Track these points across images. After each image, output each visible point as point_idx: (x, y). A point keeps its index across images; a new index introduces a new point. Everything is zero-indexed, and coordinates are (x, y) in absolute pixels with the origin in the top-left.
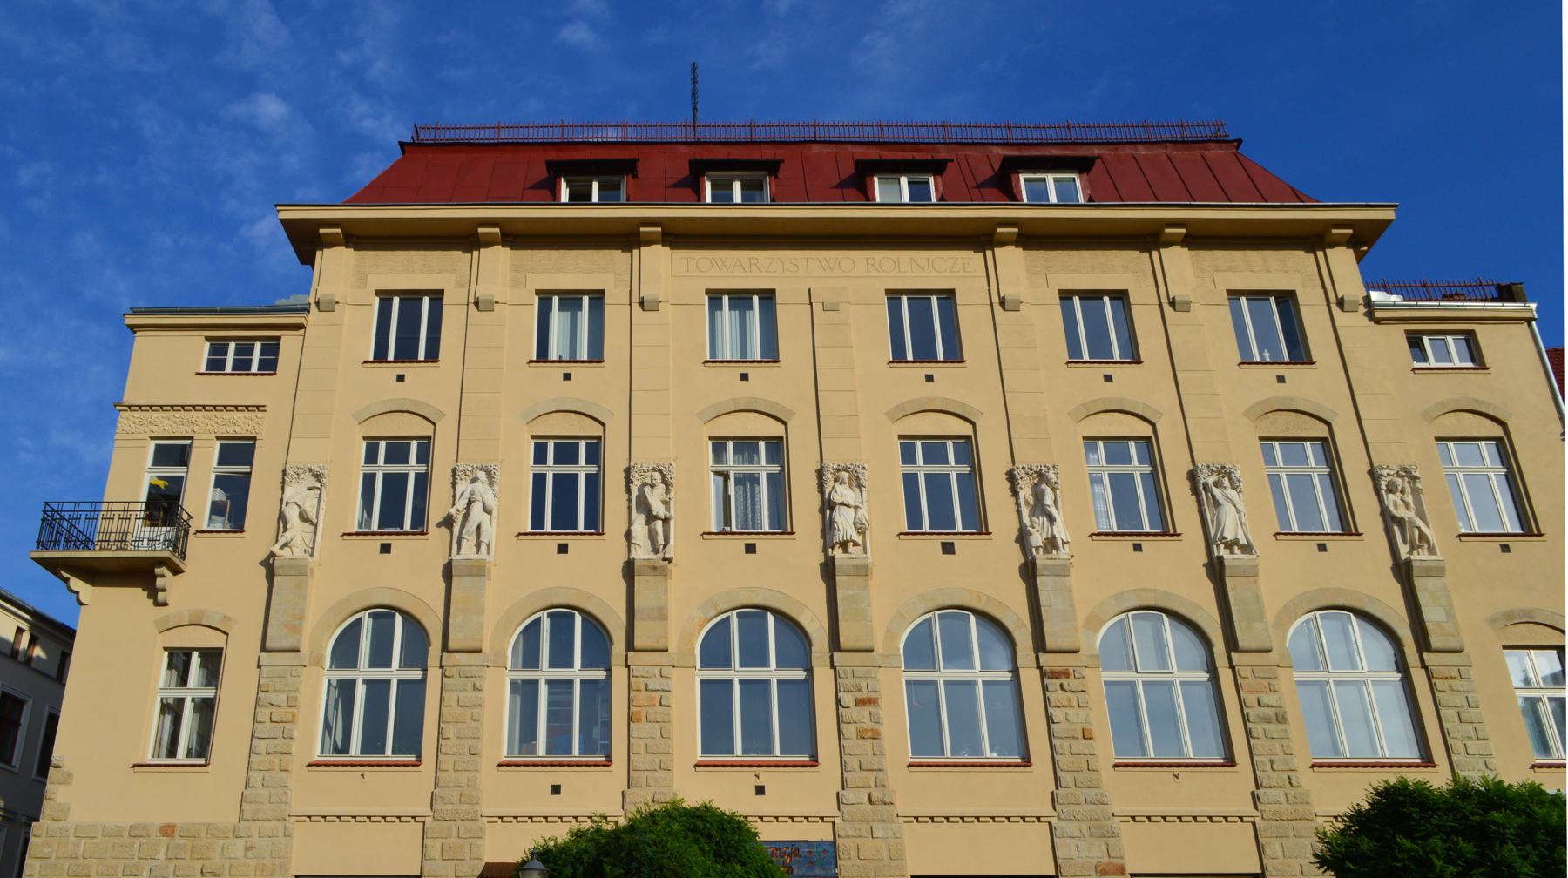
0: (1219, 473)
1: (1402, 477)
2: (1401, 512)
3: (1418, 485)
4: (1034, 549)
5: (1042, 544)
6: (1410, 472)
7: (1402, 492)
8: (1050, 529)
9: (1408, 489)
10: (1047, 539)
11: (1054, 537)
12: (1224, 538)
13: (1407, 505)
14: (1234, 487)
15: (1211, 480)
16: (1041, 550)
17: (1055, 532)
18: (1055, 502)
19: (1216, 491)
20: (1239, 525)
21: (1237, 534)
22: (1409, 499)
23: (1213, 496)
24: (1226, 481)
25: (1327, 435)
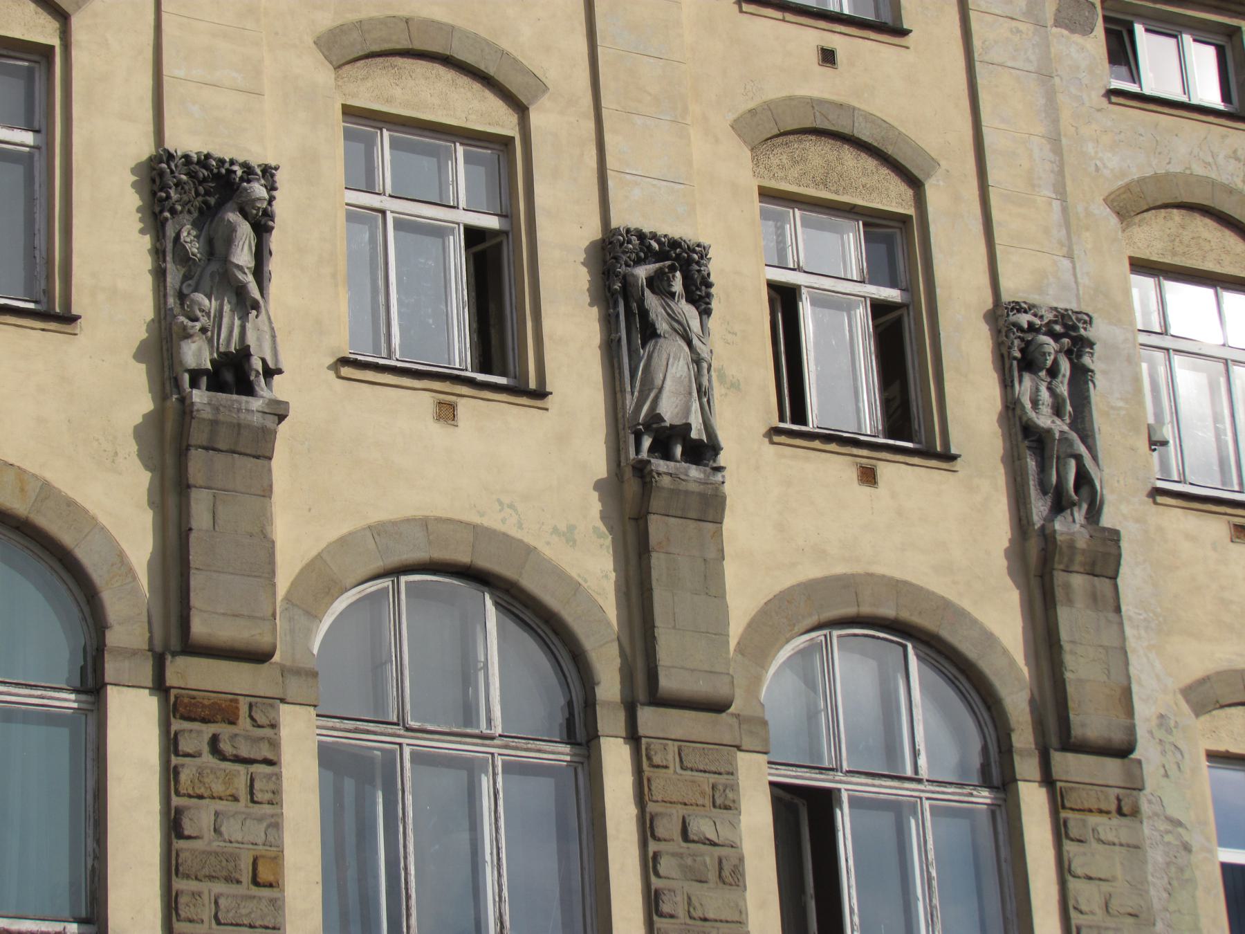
0: (660, 256)
1: (1056, 337)
2: (1044, 419)
3: (1086, 360)
4: (186, 377)
5: (209, 366)
6: (1075, 328)
7: (1053, 372)
8: (237, 322)
9: (1065, 367)
10: (226, 355)
11: (244, 353)
12: (660, 418)
13: (1058, 411)
14: (692, 299)
15: (642, 272)
16: (204, 381)
17: (251, 339)
18: (261, 254)
19: (652, 302)
20: (695, 394)
21: (687, 411)
22: (1063, 389)
23: (644, 313)
24: (677, 285)
25: (910, 211)
